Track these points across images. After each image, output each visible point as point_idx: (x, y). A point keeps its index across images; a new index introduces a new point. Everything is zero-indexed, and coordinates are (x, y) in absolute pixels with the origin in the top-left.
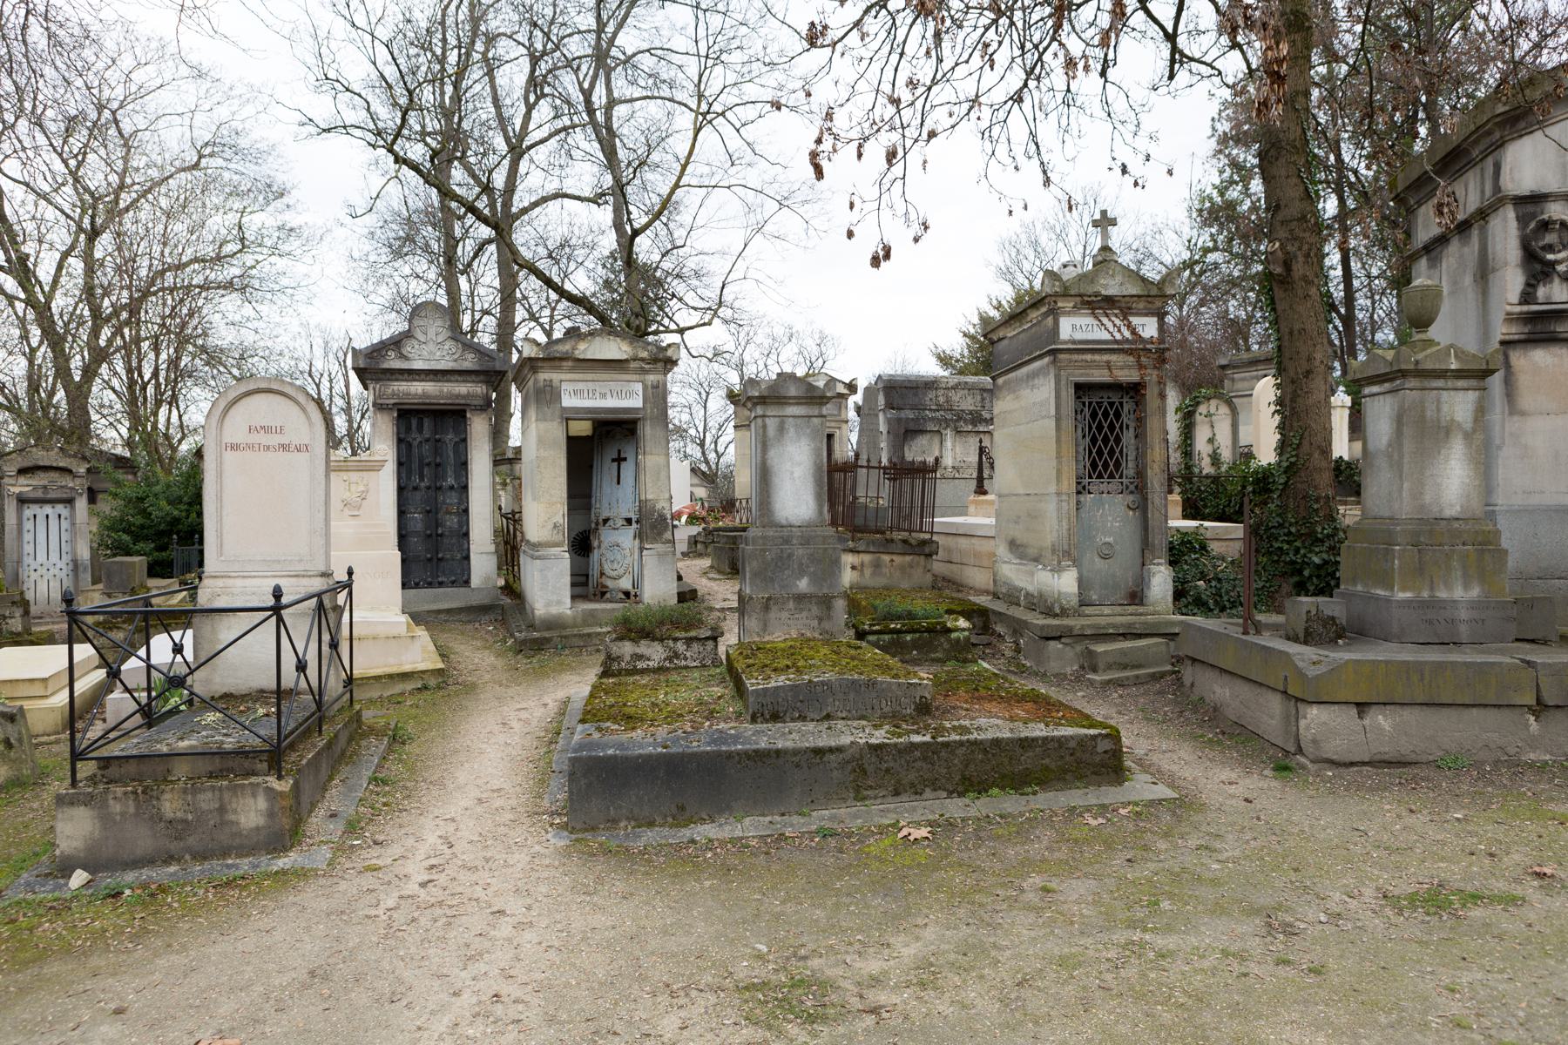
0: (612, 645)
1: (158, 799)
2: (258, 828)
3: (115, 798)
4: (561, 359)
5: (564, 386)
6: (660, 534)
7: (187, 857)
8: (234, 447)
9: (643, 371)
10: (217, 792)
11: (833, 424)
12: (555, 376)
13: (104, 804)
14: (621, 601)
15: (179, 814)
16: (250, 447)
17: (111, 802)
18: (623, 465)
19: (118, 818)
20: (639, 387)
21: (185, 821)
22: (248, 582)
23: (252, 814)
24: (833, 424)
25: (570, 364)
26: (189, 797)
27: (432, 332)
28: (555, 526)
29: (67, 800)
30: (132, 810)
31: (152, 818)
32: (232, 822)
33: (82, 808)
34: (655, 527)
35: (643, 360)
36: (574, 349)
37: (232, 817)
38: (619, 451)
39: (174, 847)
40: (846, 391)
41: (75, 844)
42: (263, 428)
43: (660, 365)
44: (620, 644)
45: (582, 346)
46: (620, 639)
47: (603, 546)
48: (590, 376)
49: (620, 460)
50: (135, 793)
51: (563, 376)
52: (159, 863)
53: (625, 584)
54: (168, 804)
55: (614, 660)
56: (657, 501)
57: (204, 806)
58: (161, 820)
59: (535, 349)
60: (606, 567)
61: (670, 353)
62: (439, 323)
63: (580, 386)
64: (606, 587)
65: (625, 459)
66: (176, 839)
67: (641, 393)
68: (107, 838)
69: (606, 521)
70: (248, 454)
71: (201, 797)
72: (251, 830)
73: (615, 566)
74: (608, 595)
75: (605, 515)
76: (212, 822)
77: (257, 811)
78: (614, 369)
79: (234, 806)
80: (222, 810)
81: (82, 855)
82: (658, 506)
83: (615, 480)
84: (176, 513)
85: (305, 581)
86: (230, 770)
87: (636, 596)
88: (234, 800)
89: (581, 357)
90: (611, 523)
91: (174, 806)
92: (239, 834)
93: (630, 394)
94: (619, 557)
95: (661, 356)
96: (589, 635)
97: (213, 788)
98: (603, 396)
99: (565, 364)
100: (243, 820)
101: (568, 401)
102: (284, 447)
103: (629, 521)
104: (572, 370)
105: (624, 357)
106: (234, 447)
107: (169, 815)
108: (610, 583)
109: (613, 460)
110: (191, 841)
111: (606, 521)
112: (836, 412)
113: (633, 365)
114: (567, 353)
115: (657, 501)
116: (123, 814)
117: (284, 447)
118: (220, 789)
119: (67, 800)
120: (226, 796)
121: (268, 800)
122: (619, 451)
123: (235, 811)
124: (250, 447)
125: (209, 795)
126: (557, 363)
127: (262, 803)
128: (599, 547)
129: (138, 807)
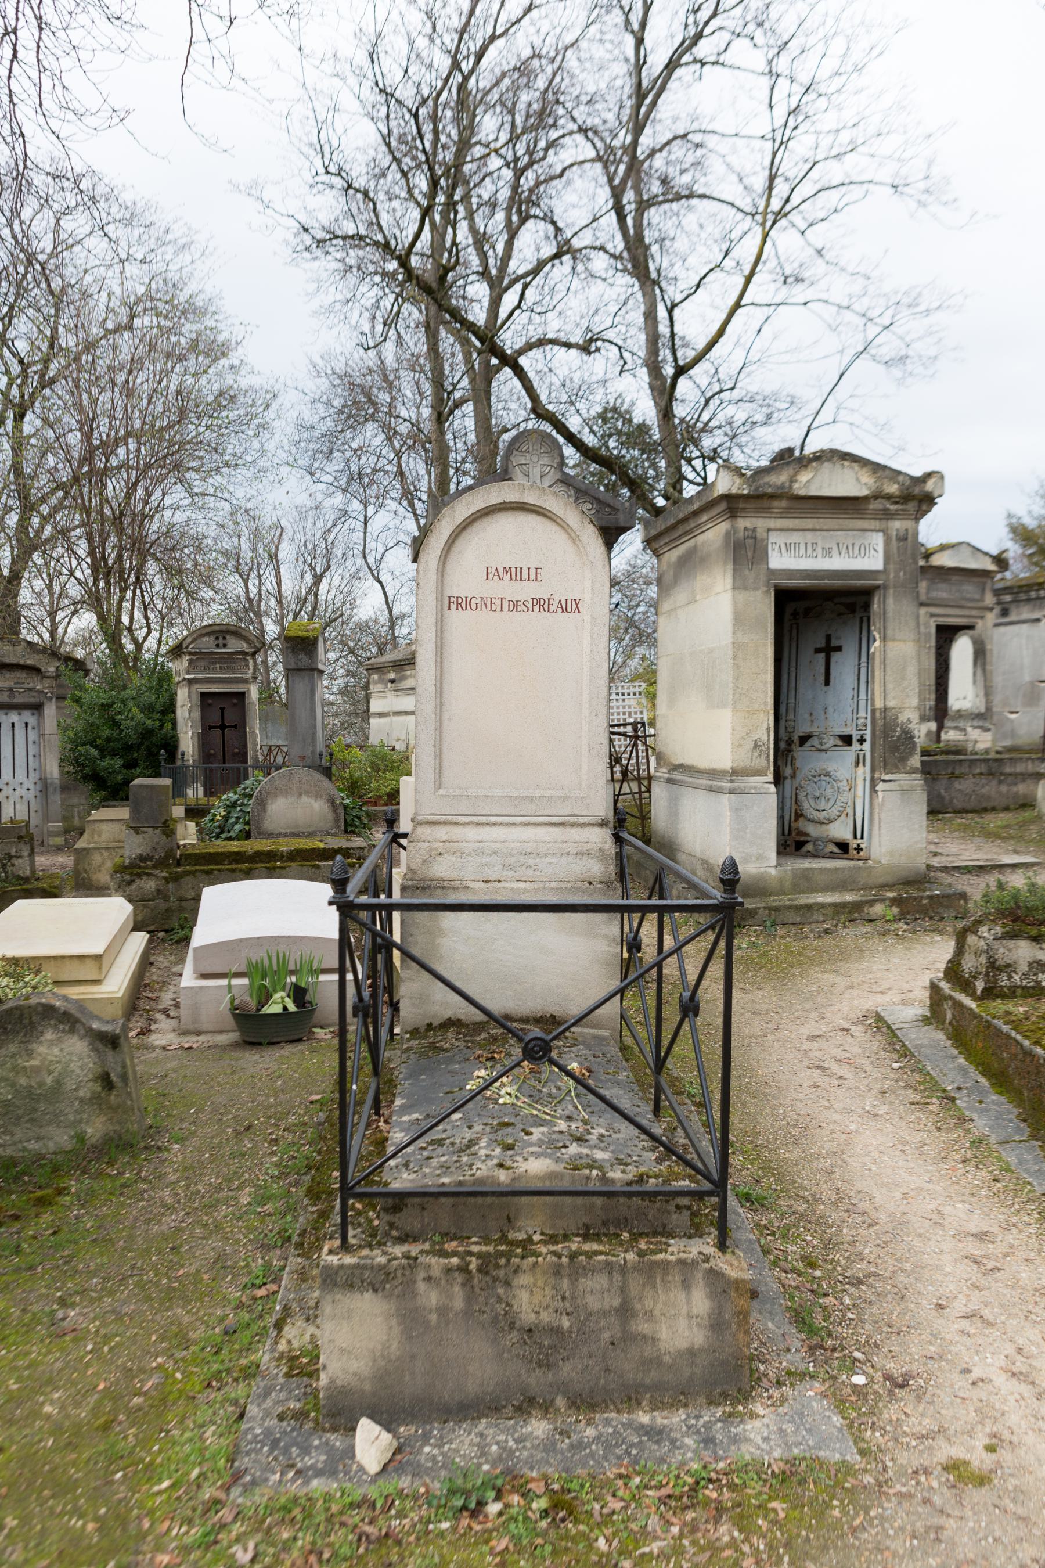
0: (996, 945)
1: (507, 1284)
2: (691, 1352)
3: (429, 1279)
4: (772, 497)
5: (774, 538)
6: (903, 759)
7: (560, 1402)
8: (464, 603)
9: (888, 515)
10: (617, 1277)
11: (974, 613)
12: (761, 524)
13: (408, 1289)
14: (832, 856)
15: (546, 1317)
16: (487, 603)
17: (421, 1286)
18: (835, 657)
19: (434, 1317)
20: (878, 540)
21: (556, 1331)
22: (485, 833)
23: (682, 1323)
24: (974, 613)
25: (784, 503)
26: (565, 1283)
27: (536, 472)
28: (756, 746)
29: (341, 1278)
30: (459, 1303)
31: (495, 1321)
32: (644, 1337)
33: (368, 1295)
34: (897, 749)
35: (889, 497)
36: (792, 480)
37: (643, 1327)
38: (828, 638)
39: (536, 1380)
40: (992, 567)
41: (355, 1365)
42: (507, 570)
43: (911, 506)
44: (1011, 944)
45: (804, 477)
46: (1013, 936)
47: (800, 776)
48: (809, 523)
49: (829, 649)
50: (464, 1269)
51: (772, 523)
52: (509, 1411)
53: (841, 831)
54: (524, 1296)
55: (1000, 969)
56: (901, 709)
57: (593, 1303)
58: (512, 1326)
59: (738, 480)
60: (806, 805)
61: (930, 486)
62: (545, 460)
63: (795, 538)
64: (807, 835)
65: (839, 649)
66: (540, 1364)
67: (880, 548)
68: (413, 1357)
69: (804, 739)
70: (484, 614)
71: (587, 1283)
72: (680, 1353)
73: (822, 805)
74: (809, 847)
75: (803, 729)
76: (606, 1335)
77: (690, 1316)
78: (845, 511)
79: (648, 1303)
80: (625, 1311)
81: (367, 1387)
82: (903, 718)
83: (822, 678)
84: (149, 722)
85: (575, 833)
86: (623, 1222)
87: (859, 849)
88: (648, 1292)
89: (802, 492)
90: (815, 741)
91: (538, 1298)
92: (657, 1361)
93: (864, 550)
94: (829, 792)
95: (917, 491)
96: (809, 907)
97: (609, 1267)
98: (827, 552)
99: (776, 503)
100: (664, 1334)
101: (780, 560)
102: (541, 604)
103: (847, 740)
104: (786, 513)
105: (864, 492)
106: (464, 603)
107: (527, 1317)
108: (812, 830)
109: (818, 651)
110: (567, 1371)
111: (804, 739)
112: (977, 596)
113: (874, 505)
114: (782, 487)
115: (901, 709)
116: (442, 1311)
117: (541, 604)
118: (623, 1269)
119: (341, 1278)
120: (635, 1283)
121: (713, 1295)
122: (828, 638)
123: (650, 1316)
124: (487, 603)
125: (601, 1280)
126: (766, 503)
127: (700, 1302)
128: (793, 776)
129: (469, 1300)
